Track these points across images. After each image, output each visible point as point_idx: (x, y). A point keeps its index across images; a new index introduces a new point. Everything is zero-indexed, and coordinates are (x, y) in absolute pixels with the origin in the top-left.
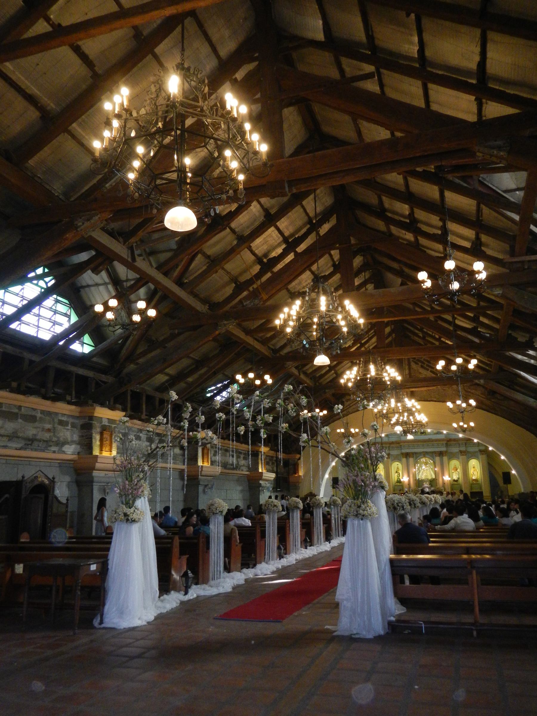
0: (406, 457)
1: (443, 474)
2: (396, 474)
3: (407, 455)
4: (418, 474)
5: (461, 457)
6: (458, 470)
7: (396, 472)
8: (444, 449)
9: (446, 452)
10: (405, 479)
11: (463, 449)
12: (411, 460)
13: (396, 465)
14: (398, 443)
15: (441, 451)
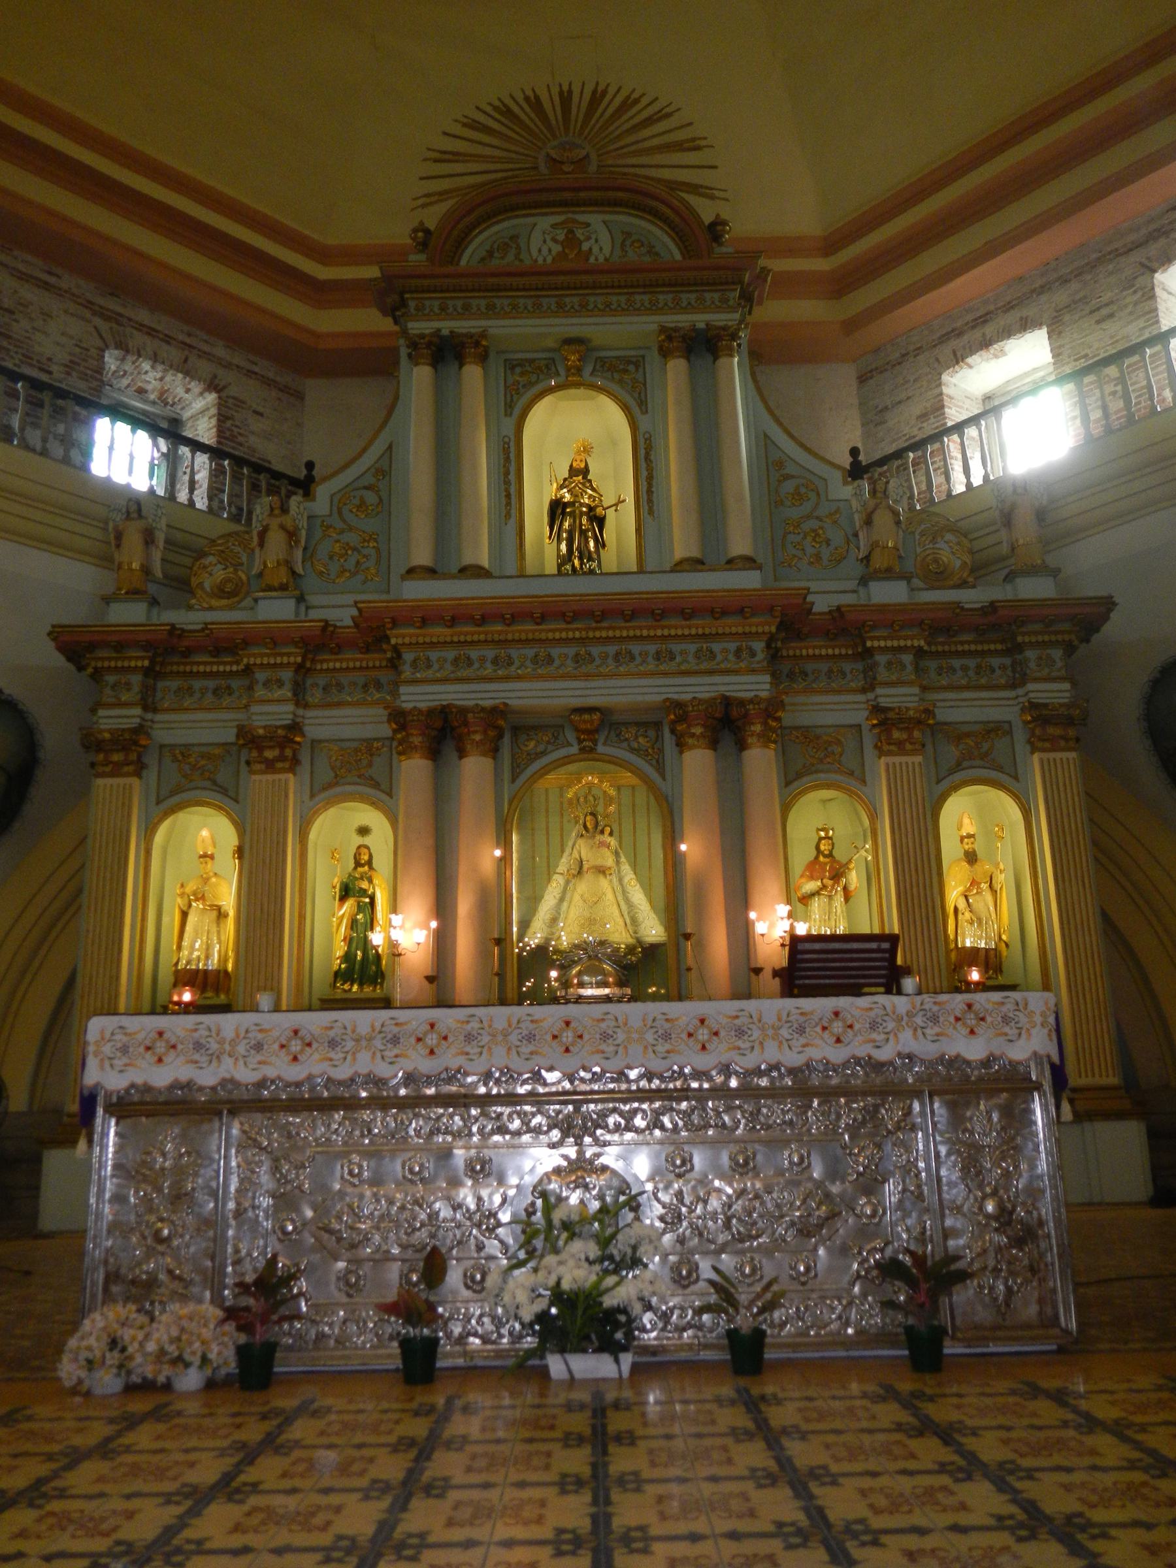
0: (434, 753)
1: (740, 898)
2: (349, 905)
3: (443, 734)
4: (525, 925)
5: (880, 768)
6: (854, 878)
7: (346, 892)
8: (752, 685)
9: (771, 709)
10: (406, 932)
11: (900, 696)
12: (474, 771)
13: (343, 831)
14: (374, 634)
15: (727, 701)
